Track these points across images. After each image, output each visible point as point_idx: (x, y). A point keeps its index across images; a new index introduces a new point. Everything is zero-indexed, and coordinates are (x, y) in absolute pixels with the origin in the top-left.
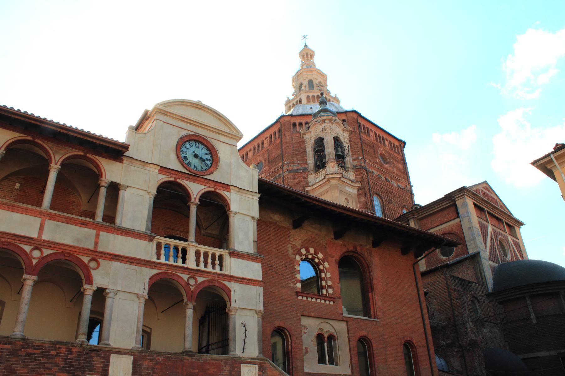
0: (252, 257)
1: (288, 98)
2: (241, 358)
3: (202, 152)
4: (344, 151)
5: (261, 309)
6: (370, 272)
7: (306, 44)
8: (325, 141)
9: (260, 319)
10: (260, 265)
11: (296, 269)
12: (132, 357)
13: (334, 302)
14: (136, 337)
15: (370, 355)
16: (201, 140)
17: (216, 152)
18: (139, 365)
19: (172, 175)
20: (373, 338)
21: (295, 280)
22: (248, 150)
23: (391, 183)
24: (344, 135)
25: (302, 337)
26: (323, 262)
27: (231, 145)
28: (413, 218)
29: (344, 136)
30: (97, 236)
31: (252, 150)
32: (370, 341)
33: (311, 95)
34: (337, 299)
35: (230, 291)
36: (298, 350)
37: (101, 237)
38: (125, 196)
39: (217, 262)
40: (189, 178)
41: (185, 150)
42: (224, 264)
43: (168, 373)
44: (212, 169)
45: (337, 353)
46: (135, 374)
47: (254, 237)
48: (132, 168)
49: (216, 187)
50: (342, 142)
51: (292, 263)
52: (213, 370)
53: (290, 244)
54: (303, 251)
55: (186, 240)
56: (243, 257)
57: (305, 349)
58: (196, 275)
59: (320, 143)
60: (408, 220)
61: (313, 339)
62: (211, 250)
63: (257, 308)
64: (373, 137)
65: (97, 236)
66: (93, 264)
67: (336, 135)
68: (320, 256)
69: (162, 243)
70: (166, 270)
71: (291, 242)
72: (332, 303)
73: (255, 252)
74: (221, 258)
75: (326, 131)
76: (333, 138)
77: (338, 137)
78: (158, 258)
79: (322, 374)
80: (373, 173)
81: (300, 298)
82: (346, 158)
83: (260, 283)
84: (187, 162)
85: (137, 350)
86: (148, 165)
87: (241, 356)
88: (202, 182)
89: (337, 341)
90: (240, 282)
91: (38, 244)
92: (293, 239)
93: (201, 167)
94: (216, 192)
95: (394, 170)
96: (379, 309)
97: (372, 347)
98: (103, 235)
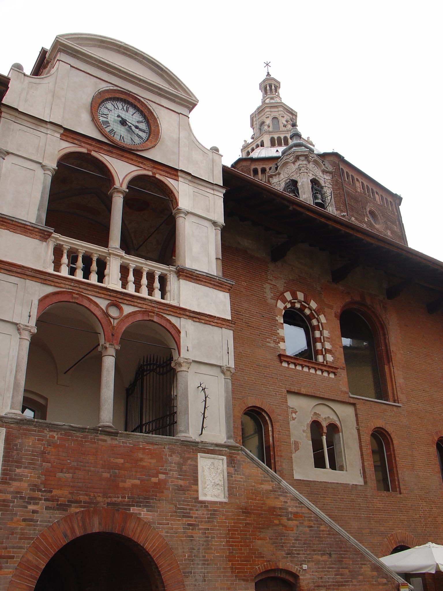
0: (215, 282)
1: (245, 141)
2: (198, 443)
4: (325, 198)
5: (229, 366)
6: (384, 334)
7: (268, 73)
8: (299, 184)
9: (230, 382)
11: (277, 321)
13: (335, 374)
14: (13, 397)
15: (389, 456)
16: (131, 100)
17: (155, 119)
18: (16, 445)
19: (83, 145)
20: (393, 431)
21: (277, 338)
24: (325, 177)
25: (289, 424)
26: (317, 314)
27: (179, 114)
29: (324, 178)
32: (389, 435)
34: (339, 370)
35: (180, 333)
36: (284, 445)
39: (157, 284)
40: (112, 152)
41: (106, 111)
42: (168, 288)
43: (69, 461)
45: (341, 452)
46: (8, 461)
47: (217, 253)
49: (155, 170)
50: (322, 187)
51: (271, 313)
52: (150, 461)
53: (269, 283)
54: (288, 296)
55: (106, 245)
56: (199, 280)
57: (295, 443)
58: (120, 301)
59: (293, 188)
61: (305, 429)
63: (224, 363)
67: (314, 177)
68: (313, 305)
69: (64, 246)
70: (69, 289)
71: (269, 281)
72: (332, 376)
74: (163, 280)
75: (301, 171)
76: (310, 181)
81: (285, 365)
82: (328, 207)
83: (228, 324)
84: (108, 130)
85: (14, 419)
86: (44, 125)
87: (198, 439)
88: (132, 160)
89: (341, 434)
90: (195, 319)
92: (273, 277)
93: (132, 139)
94: (155, 177)
95: (387, 233)
96: (400, 389)
97: (393, 444)
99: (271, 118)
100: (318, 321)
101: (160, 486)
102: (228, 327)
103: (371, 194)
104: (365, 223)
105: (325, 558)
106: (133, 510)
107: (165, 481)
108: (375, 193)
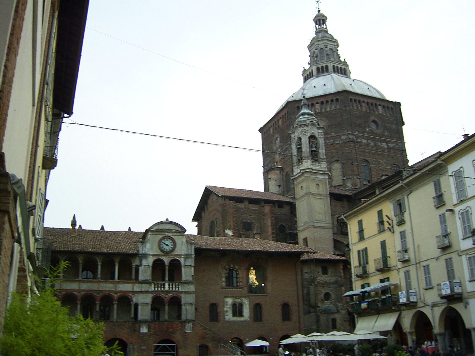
3: (168, 242)
16: (169, 237)
22: (270, 126)
23: (381, 145)
28: (378, 187)
31: (272, 126)
33: (320, 66)
35: (181, 297)
60: (375, 189)
64: (364, 107)
66: (133, 296)
67: (311, 134)
68: (237, 267)
72: (241, 290)
77: (314, 136)
80: (361, 142)
81: (224, 289)
104: (367, 132)
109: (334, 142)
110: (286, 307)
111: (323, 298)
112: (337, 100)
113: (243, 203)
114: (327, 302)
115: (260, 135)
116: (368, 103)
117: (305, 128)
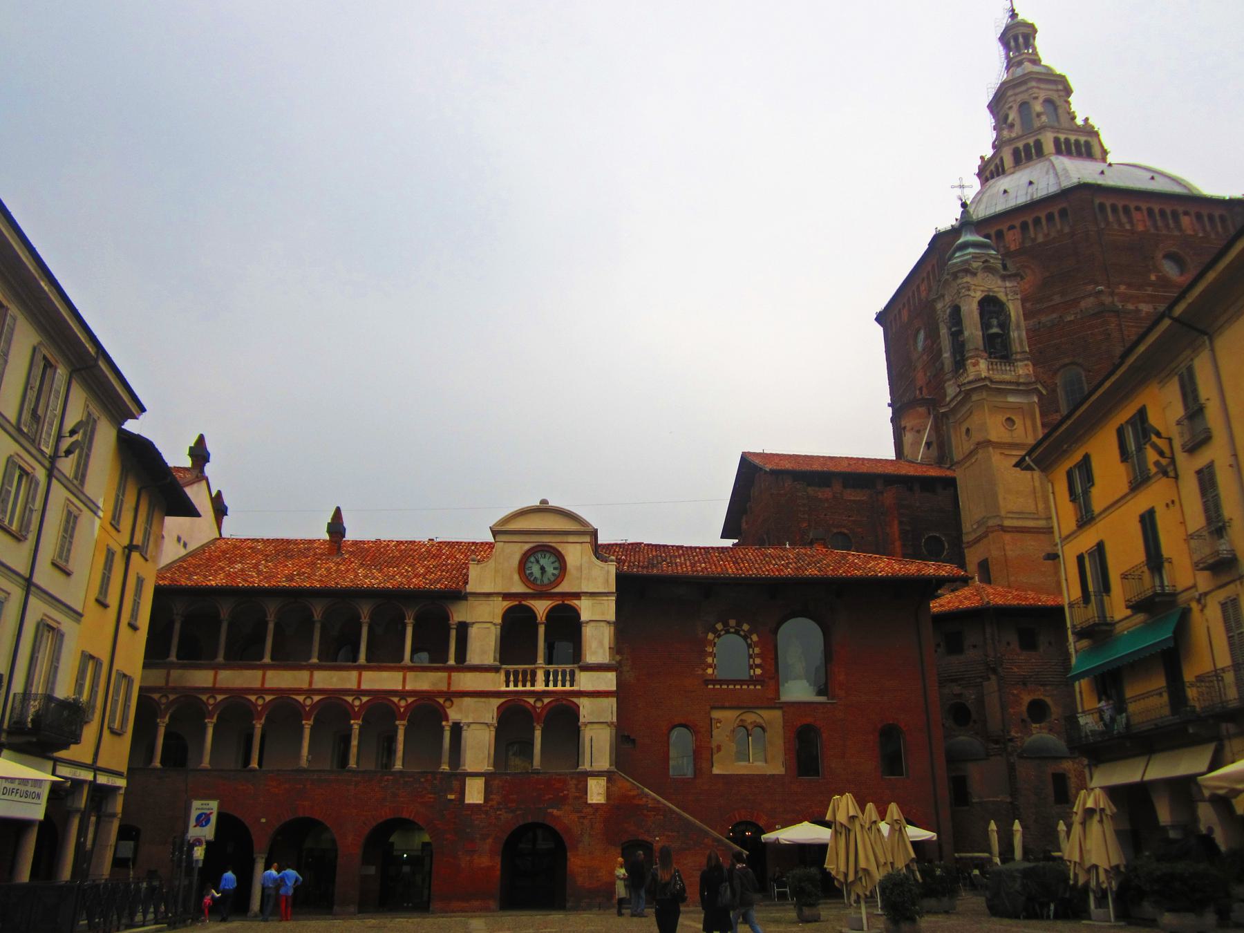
3: (547, 562)
10: (614, 673)
11: (706, 651)
12: (484, 778)
13: (762, 686)
16: (546, 549)
19: (517, 599)
27: (582, 543)
29: (1006, 288)
30: (450, 677)
33: (1020, 145)
35: (579, 707)
37: (453, 678)
38: (473, 632)
44: (559, 579)
48: (477, 603)
54: (719, 626)
61: (728, 734)
62: (560, 667)
63: (609, 720)
65: (450, 677)
66: (448, 704)
67: (986, 293)
68: (746, 627)
72: (759, 687)
73: (610, 660)
74: (572, 674)
75: (961, 295)
77: (993, 296)
78: (508, 686)
79: (737, 775)
80: (1137, 311)
91: (403, 694)
98: (455, 675)
99: (1015, 107)
100: (751, 639)
101: (565, 798)
102: (612, 696)
103: (1171, 222)
104: (1151, 284)
105: (675, 834)
106: (550, 810)
107: (568, 794)
108: (1181, 215)
109: (1060, 317)
110: (889, 734)
111: (1025, 716)
112: (1063, 213)
113: (829, 486)
114: (1038, 725)
115: (879, 330)
116: (1150, 212)
117: (968, 279)
